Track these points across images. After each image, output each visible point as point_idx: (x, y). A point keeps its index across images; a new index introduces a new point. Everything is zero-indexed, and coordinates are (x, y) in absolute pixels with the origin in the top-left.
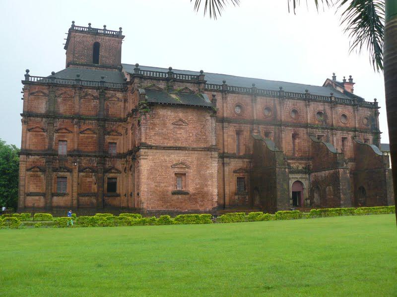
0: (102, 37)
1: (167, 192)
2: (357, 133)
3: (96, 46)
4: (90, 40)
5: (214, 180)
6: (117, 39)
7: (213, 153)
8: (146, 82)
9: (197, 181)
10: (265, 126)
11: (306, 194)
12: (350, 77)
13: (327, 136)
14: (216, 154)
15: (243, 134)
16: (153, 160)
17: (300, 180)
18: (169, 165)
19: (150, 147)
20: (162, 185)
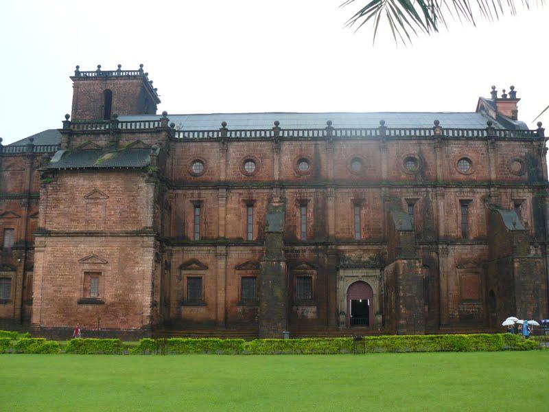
0: (116, 81)
1: (71, 300)
2: (492, 189)
3: (108, 95)
4: (99, 88)
5: (145, 281)
6: (135, 81)
7: (146, 239)
8: (78, 139)
9: (119, 284)
10: (297, 190)
11: (374, 304)
12: (512, 88)
13: (426, 201)
14: (150, 241)
15: (256, 207)
16: (52, 252)
17: (364, 280)
18: (76, 259)
19: (48, 234)
20: (63, 289)
